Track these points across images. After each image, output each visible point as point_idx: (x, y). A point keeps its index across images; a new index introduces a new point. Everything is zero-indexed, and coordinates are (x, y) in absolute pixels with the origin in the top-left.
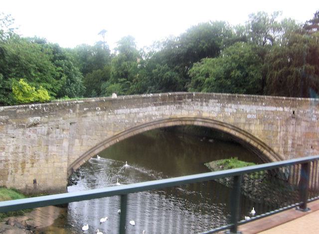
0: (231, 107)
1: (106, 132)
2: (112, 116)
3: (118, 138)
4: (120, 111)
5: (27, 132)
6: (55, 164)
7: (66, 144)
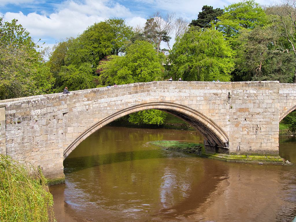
0: (185, 92)
3: (101, 124)
4: (103, 100)
6: (54, 150)
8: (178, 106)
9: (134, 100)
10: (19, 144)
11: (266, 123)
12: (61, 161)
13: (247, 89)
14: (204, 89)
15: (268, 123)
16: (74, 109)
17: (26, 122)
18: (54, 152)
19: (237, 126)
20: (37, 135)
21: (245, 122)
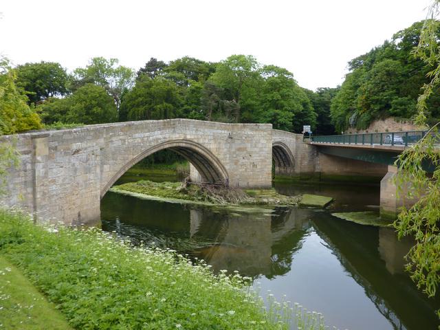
2: (132, 140)
4: (137, 135)
5: (73, 160)
7: (98, 170)
9: (164, 136)
12: (98, 204)
15: (263, 161)
16: (110, 145)
17: (68, 157)
19: (236, 164)
21: (244, 161)
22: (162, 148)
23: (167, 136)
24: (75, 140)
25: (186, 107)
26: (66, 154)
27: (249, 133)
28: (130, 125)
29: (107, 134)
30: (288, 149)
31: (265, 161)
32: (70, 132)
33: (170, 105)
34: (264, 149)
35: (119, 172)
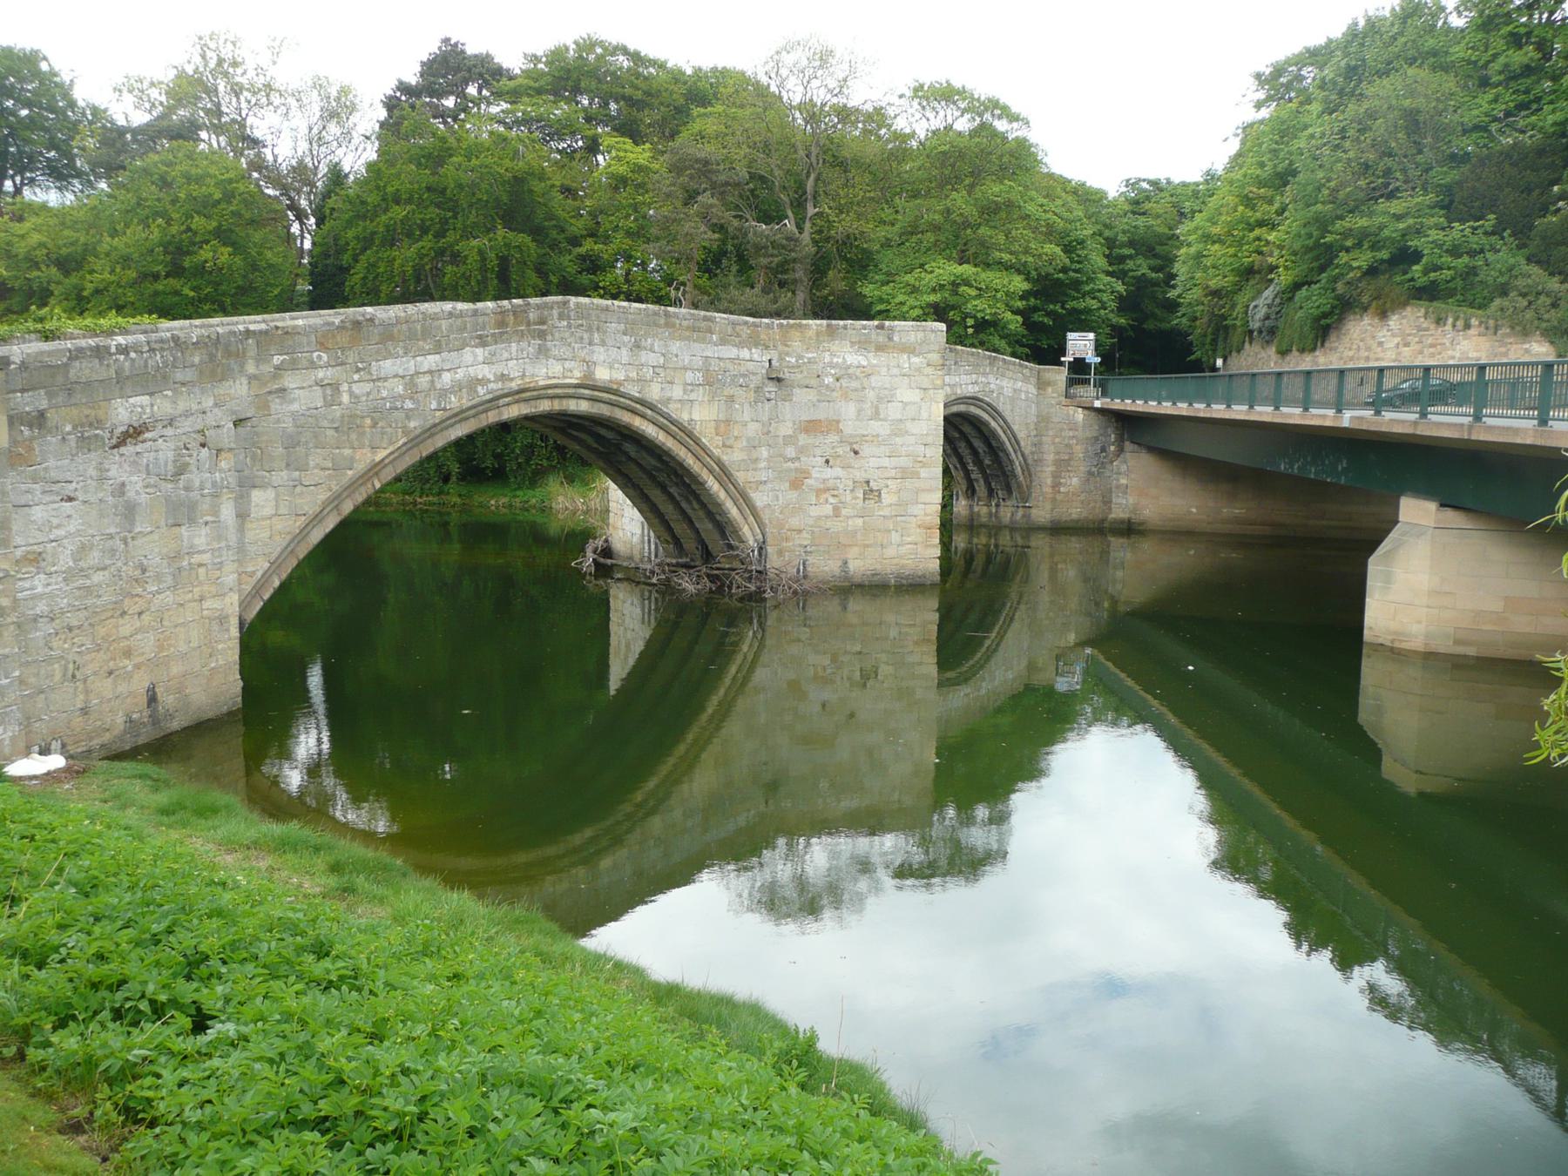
1: (347, 452)
2: (367, 387)
4: (388, 363)
5: (119, 468)
6: (206, 604)
7: (227, 511)
8: (628, 402)
9: (499, 368)
10: (65, 580)
11: (899, 475)
13: (835, 346)
14: (703, 341)
15: (905, 474)
16: (276, 405)
18: (205, 612)
19: (796, 484)
20: (139, 529)
21: (829, 473)
22: (492, 417)
23: (513, 369)
24: (126, 383)
25: (588, 246)
26: (86, 443)
27: (853, 358)
28: (357, 324)
29: (260, 359)
30: (1007, 427)
31: (916, 475)
32: (100, 353)
33: (524, 239)
34: (909, 425)
35: (317, 518)
